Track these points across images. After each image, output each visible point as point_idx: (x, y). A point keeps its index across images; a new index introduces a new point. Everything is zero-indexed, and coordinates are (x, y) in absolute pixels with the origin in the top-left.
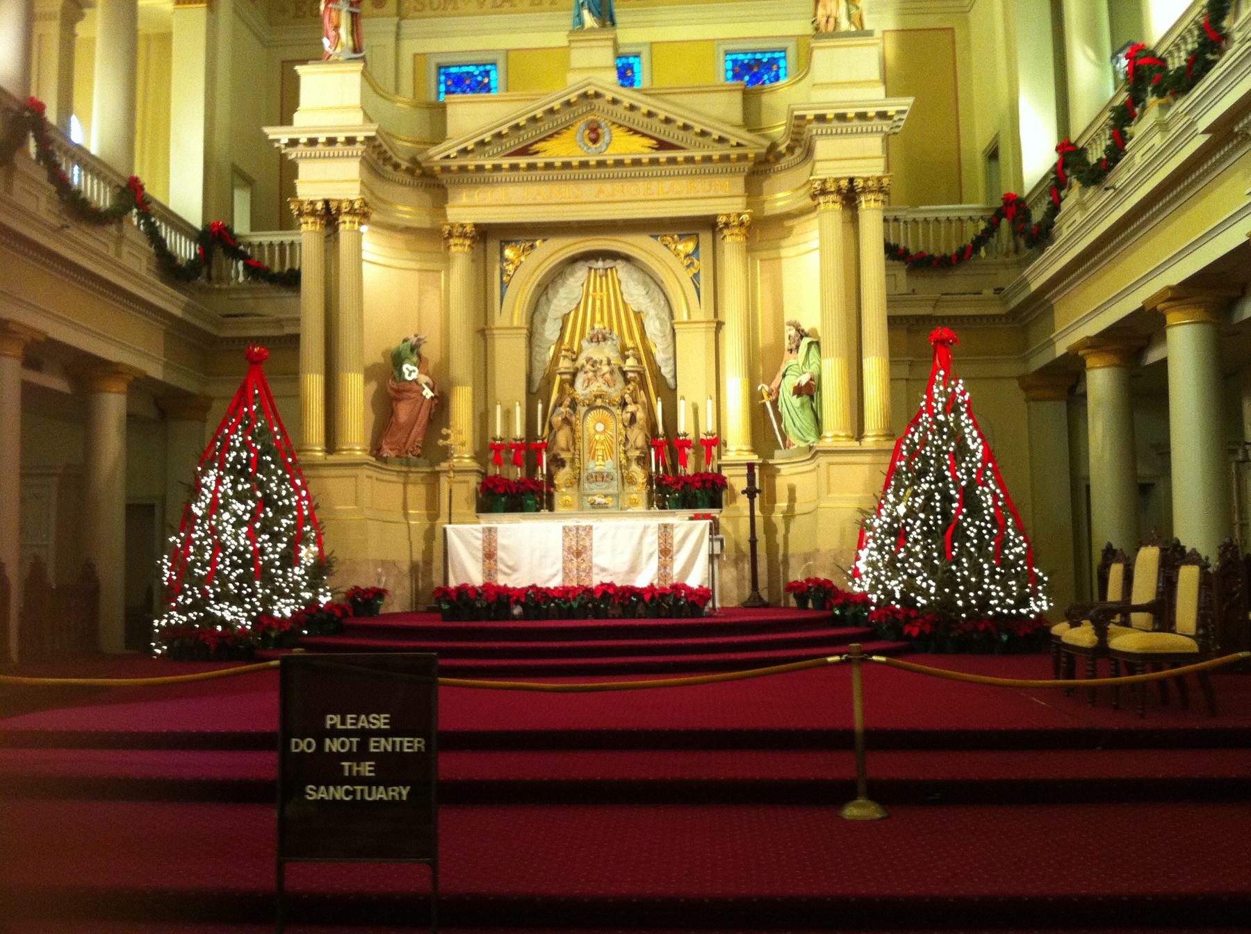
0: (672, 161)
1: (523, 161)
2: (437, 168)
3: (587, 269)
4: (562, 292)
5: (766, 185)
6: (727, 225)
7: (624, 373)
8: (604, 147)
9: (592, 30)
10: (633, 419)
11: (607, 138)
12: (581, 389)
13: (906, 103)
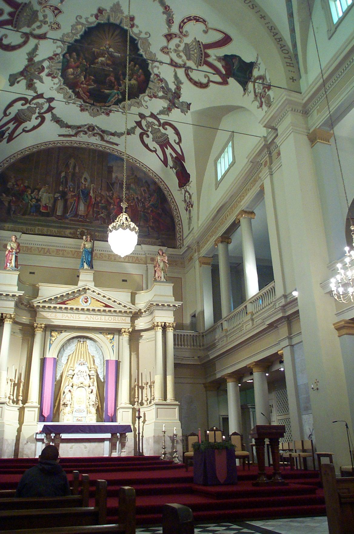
0: (110, 311)
2: (35, 306)
3: (77, 341)
4: (69, 348)
5: (136, 321)
6: (125, 332)
7: (90, 376)
8: (89, 304)
9: (86, 269)
10: (92, 392)
11: (89, 302)
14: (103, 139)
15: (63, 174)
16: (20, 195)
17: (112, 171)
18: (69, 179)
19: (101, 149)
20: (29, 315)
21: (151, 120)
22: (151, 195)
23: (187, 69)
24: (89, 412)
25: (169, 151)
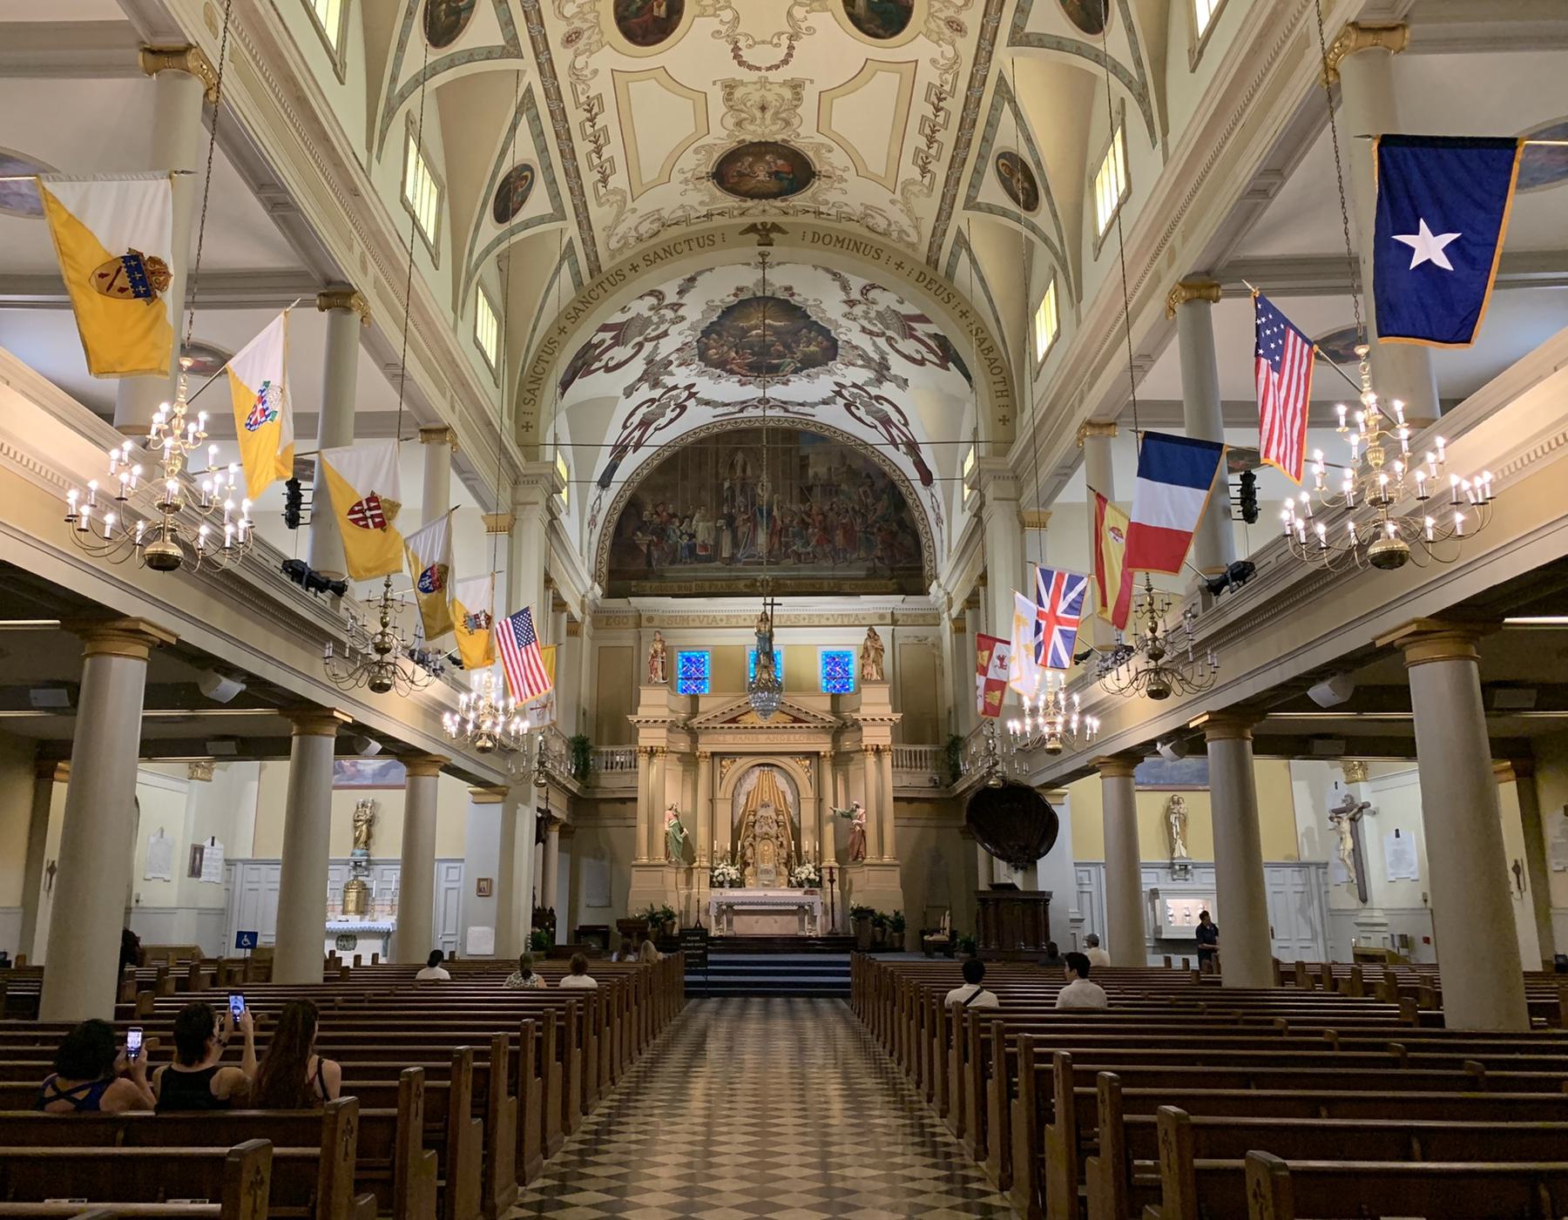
1: (734, 725)
10: (782, 845)
12: (757, 830)
13: (899, 715)
14: (787, 411)
15: (727, 485)
16: (661, 532)
17: (808, 465)
18: (738, 492)
19: (786, 425)
20: (689, 739)
21: (856, 391)
22: (878, 499)
23: (889, 340)
24: (779, 874)
25: (894, 432)
